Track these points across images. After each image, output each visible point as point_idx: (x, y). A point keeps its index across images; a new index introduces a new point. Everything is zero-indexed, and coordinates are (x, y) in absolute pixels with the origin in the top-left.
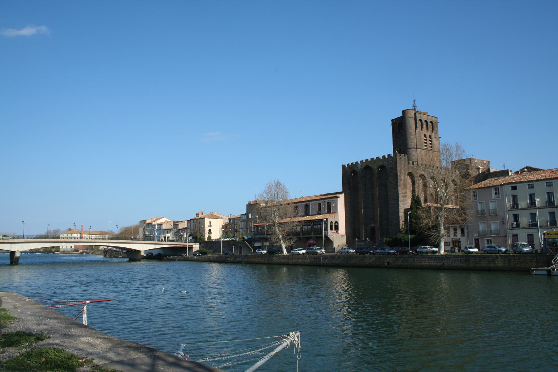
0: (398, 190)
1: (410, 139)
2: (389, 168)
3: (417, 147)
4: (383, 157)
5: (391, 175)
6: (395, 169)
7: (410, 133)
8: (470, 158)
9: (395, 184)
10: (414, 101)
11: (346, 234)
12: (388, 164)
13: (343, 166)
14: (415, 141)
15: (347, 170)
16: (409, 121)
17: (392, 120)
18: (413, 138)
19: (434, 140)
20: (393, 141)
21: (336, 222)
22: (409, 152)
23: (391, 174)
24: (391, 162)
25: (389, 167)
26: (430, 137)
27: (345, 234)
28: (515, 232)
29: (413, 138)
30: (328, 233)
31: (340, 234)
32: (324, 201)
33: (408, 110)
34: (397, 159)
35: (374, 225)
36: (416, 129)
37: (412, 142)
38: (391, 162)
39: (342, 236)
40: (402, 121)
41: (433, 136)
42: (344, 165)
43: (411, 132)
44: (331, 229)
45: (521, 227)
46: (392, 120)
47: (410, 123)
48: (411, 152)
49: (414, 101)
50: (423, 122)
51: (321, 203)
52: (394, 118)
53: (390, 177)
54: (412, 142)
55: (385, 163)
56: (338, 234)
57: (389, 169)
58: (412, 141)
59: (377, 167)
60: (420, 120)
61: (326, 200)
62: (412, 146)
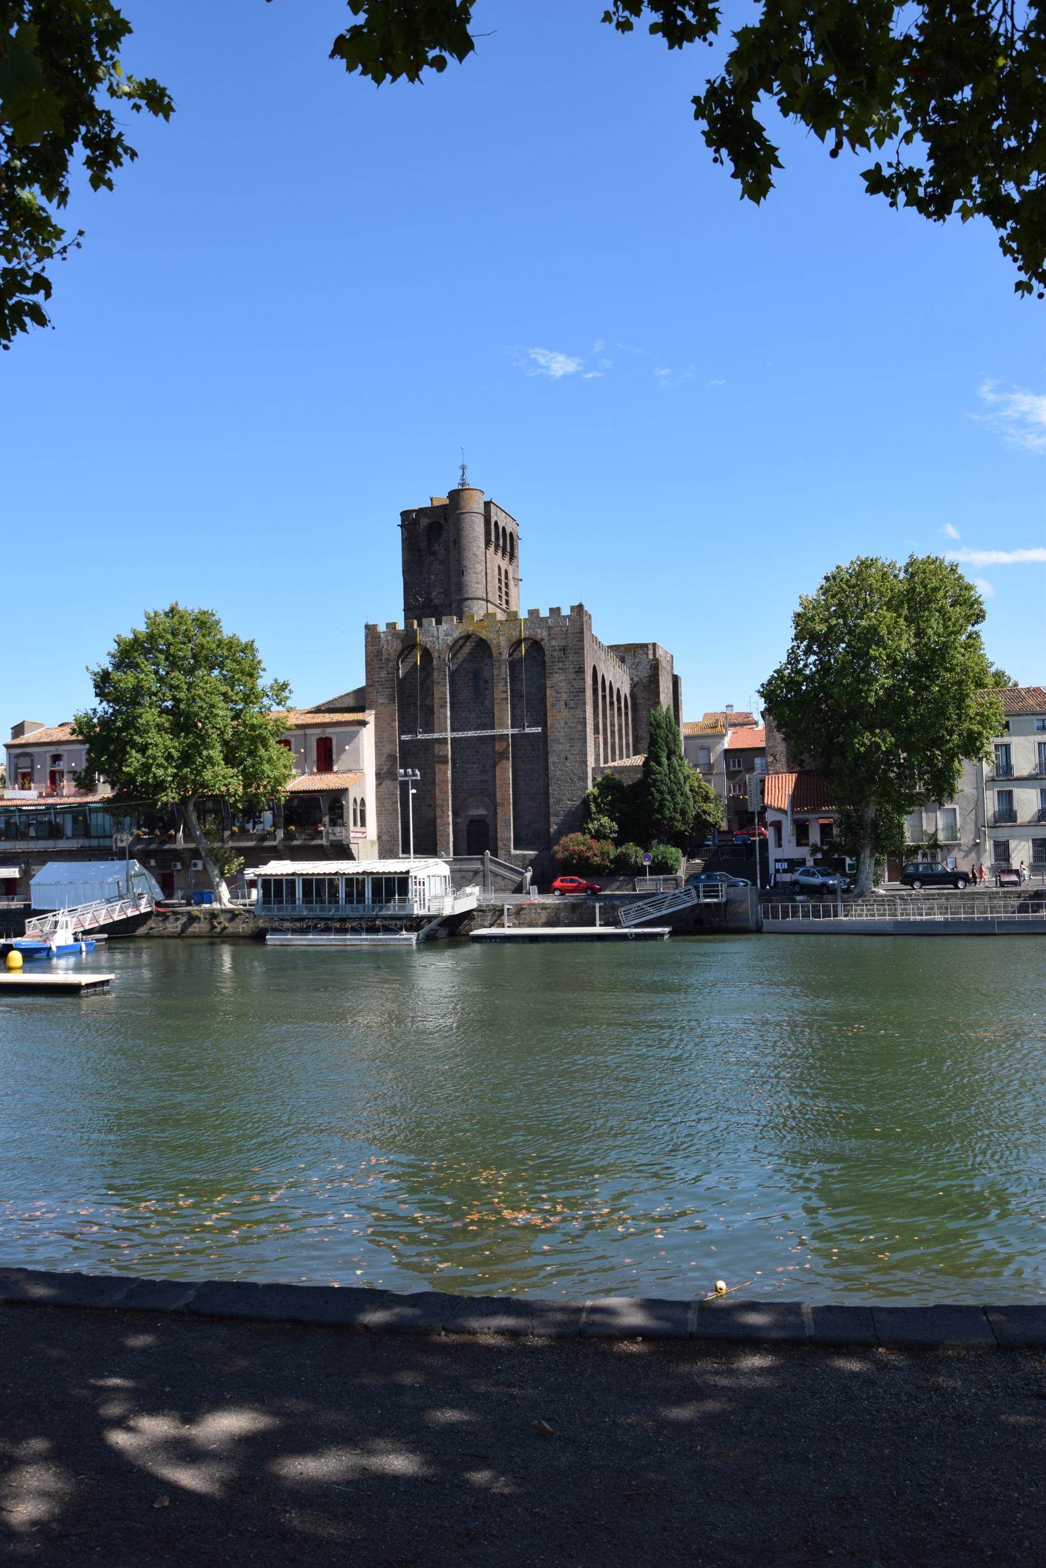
0: (585, 711)
1: (475, 573)
2: (554, 646)
3: (490, 598)
4: (555, 611)
5: (559, 669)
6: (575, 653)
7: (475, 555)
8: (654, 644)
9: (574, 696)
10: (463, 468)
11: (379, 837)
12: (549, 635)
13: (370, 630)
14: (484, 579)
15: (388, 641)
16: (473, 522)
17: (405, 515)
18: (481, 572)
19: (511, 583)
20: (405, 572)
21: (362, 800)
22: (471, 609)
23: (560, 665)
24: (561, 630)
25: (554, 643)
26: (506, 572)
27: (375, 838)
28: (1002, 834)
29: (481, 572)
30: (348, 837)
31: (368, 838)
32: (305, 735)
33: (474, 492)
34: (583, 625)
35: (484, 813)
36: (486, 548)
37: (479, 581)
38: (561, 630)
39: (372, 842)
40: (446, 520)
41: (510, 575)
42: (375, 626)
43: (477, 552)
44: (355, 824)
45: (1019, 821)
46: (405, 515)
47: (475, 526)
48: (475, 609)
49: (463, 468)
50: (501, 530)
51: (293, 740)
52: (417, 508)
53: (556, 673)
54: (478, 583)
55: (542, 634)
56: (365, 837)
57: (554, 651)
58: (478, 578)
59: (509, 640)
60: (496, 523)
61: (308, 731)
62: (481, 594)
